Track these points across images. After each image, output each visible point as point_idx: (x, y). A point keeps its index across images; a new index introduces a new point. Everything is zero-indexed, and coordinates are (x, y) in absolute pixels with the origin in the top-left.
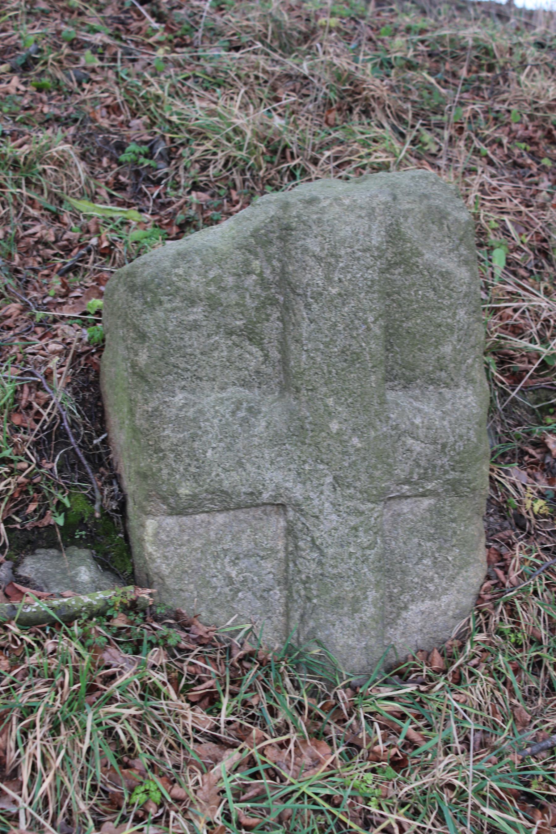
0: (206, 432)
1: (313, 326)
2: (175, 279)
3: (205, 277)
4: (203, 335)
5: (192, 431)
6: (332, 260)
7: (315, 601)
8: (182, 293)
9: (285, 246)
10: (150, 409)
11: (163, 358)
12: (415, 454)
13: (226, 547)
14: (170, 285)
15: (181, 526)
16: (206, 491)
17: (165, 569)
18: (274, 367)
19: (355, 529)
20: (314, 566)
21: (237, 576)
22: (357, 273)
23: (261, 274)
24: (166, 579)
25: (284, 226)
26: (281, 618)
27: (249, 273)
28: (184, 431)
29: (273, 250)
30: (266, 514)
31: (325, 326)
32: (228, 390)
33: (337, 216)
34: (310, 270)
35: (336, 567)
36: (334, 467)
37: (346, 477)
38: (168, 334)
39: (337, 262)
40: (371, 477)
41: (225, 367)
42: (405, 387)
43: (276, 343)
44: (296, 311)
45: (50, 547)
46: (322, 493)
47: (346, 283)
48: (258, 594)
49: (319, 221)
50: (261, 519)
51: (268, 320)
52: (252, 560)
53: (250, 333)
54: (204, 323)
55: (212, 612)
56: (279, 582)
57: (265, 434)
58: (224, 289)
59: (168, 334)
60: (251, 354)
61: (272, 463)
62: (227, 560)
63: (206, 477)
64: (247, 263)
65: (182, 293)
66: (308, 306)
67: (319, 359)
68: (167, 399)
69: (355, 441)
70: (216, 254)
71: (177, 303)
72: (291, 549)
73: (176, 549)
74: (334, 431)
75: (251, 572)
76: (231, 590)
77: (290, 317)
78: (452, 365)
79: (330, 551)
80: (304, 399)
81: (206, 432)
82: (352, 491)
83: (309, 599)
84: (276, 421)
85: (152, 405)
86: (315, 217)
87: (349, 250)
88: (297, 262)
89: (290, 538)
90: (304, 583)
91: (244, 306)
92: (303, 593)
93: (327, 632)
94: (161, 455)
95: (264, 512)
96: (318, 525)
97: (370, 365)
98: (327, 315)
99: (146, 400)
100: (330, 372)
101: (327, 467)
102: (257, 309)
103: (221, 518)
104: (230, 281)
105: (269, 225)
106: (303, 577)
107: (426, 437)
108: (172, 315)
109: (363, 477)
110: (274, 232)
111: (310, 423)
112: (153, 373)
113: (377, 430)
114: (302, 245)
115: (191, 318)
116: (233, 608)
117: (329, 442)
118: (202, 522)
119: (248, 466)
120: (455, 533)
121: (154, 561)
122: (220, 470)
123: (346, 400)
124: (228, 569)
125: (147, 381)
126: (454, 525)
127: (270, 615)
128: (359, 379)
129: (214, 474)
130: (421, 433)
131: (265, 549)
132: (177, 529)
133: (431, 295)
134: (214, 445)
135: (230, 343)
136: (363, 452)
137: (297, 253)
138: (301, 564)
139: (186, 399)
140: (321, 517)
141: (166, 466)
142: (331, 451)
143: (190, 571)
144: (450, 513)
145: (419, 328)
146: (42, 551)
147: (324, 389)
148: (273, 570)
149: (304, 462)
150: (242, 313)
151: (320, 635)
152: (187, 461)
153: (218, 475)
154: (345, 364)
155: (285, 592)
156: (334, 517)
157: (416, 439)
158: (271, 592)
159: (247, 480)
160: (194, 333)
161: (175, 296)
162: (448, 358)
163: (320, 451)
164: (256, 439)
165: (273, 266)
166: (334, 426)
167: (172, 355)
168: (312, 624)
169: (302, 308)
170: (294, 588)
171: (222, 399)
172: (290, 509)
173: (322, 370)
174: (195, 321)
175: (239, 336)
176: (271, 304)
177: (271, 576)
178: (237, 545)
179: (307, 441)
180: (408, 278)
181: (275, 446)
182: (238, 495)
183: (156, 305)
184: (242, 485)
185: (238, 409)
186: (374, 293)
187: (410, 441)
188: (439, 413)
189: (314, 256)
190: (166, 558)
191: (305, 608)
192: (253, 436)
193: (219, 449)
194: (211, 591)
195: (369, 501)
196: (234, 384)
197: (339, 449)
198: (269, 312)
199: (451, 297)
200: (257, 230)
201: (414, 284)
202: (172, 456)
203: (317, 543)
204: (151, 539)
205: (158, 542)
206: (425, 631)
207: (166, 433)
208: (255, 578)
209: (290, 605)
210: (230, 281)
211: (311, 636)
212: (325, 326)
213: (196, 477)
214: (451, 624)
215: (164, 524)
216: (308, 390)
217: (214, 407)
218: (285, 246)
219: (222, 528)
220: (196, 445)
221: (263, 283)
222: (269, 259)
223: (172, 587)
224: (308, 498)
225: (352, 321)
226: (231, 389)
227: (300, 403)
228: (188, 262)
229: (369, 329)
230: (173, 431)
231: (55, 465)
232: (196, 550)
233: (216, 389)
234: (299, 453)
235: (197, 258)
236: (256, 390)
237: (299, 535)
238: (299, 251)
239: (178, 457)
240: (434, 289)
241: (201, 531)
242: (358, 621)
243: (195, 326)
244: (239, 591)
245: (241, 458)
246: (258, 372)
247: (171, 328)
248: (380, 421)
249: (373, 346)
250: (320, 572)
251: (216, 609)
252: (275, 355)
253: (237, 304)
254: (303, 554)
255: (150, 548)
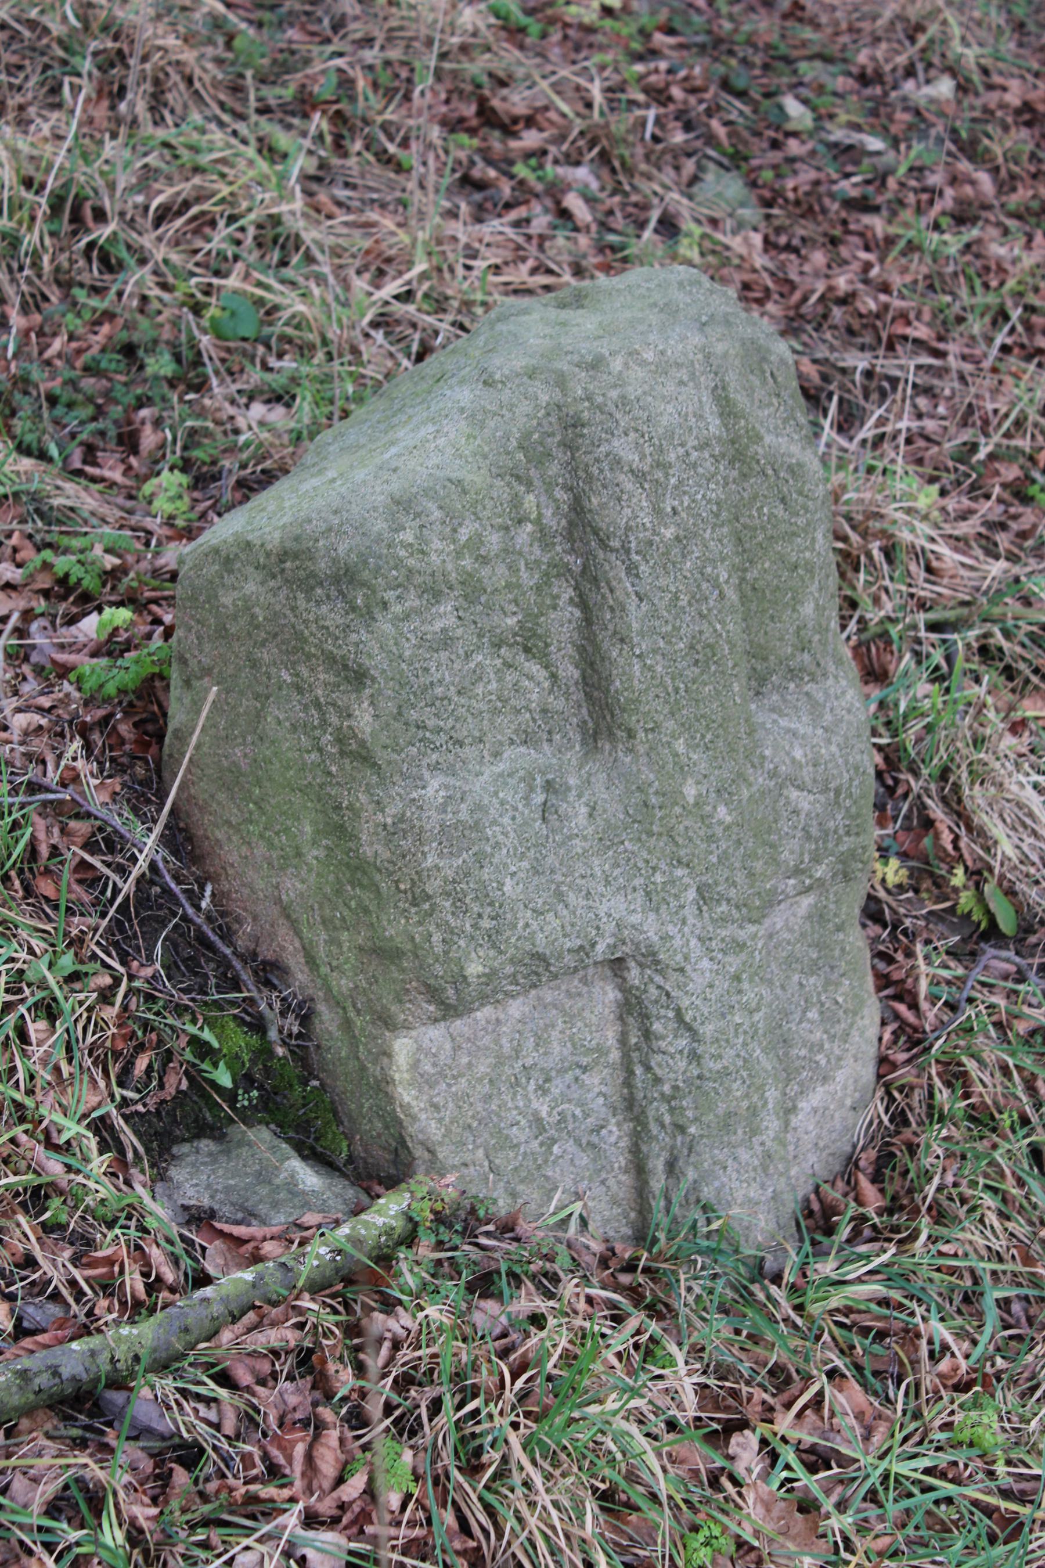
0: (497, 845)
1: (645, 607)
2: (403, 553)
3: (454, 542)
4: (458, 656)
5: (475, 849)
6: (659, 475)
7: (692, 1130)
8: (418, 580)
9: (573, 458)
10: (389, 821)
11: (400, 714)
12: (803, 816)
13: (529, 1062)
14: (396, 568)
15: (453, 1040)
16: (512, 961)
17: (434, 1131)
18: (567, 695)
19: (737, 978)
20: (682, 1064)
21: (550, 1114)
22: (697, 493)
23: (538, 521)
24: (438, 1149)
25: (570, 421)
26: (623, 1178)
27: (520, 522)
28: (460, 851)
29: (554, 469)
30: (586, 984)
31: (662, 602)
32: (505, 755)
33: (646, 387)
34: (629, 500)
35: (720, 1057)
36: (698, 869)
37: (716, 884)
38: (404, 666)
39: (667, 475)
40: (751, 875)
41: (495, 712)
42: (758, 693)
43: (570, 650)
44: (614, 583)
45: (198, 1136)
46: (684, 922)
47: (684, 515)
48: (584, 1141)
49: (623, 402)
50: (579, 995)
51: (555, 608)
52: (569, 1076)
53: (526, 639)
54: (459, 632)
55: (514, 1195)
56: (615, 1109)
57: (590, 830)
58: (484, 560)
59: (404, 666)
60: (530, 678)
61: (608, 883)
62: (532, 1086)
63: (509, 933)
64: (516, 502)
65: (418, 580)
66: (632, 570)
67: (659, 668)
68: (414, 795)
69: (722, 811)
70: (465, 492)
71: (413, 601)
72: (634, 1040)
73: (449, 1085)
74: (691, 800)
75: (570, 1101)
76: (541, 1145)
77: (603, 596)
78: (817, 637)
79: (707, 1030)
80: (642, 749)
81: (497, 845)
82: (724, 907)
83: (682, 1129)
84: (605, 801)
85: (391, 810)
86: (614, 394)
87: (681, 451)
88: (605, 487)
89: (630, 1020)
90: (666, 1099)
91: (519, 586)
92: (667, 1119)
93: (717, 1184)
94: (426, 906)
95: (584, 981)
96: (686, 985)
97: (730, 664)
98: (662, 582)
99: (378, 803)
100: (677, 690)
101: (687, 871)
102: (538, 589)
103: (516, 1008)
104: (494, 540)
105: (545, 422)
106: (667, 1088)
107: (815, 781)
108: (405, 627)
109: (740, 877)
110: (552, 435)
111: (657, 793)
112: (385, 747)
113: (750, 785)
114: (607, 455)
115: (438, 625)
116: (547, 1178)
117: (686, 823)
118: (488, 1022)
119: (572, 898)
120: (843, 950)
121: (414, 1118)
122: (529, 913)
123: (703, 736)
124: (535, 1105)
125: (375, 764)
126: (841, 936)
127: (604, 1175)
128: (718, 693)
129: (520, 925)
130: (807, 774)
131: (591, 1050)
132: (448, 1046)
133: (780, 511)
134: (513, 869)
135: (498, 662)
136: (735, 829)
137: (601, 471)
138: (660, 1065)
139: (447, 787)
140: (688, 968)
141: (438, 926)
142: (690, 840)
143: (475, 1124)
144: (836, 915)
145: (769, 578)
146: (185, 1148)
147: (670, 725)
148: (604, 1089)
149: (654, 869)
150: (516, 602)
151: (707, 1193)
152: (476, 908)
153: (527, 925)
154: (697, 670)
155: (628, 1126)
156: (705, 964)
157: (800, 788)
158: (604, 1132)
159: (573, 925)
160: (444, 655)
161: (406, 588)
162: (810, 625)
163: (676, 844)
164: (576, 841)
165: (556, 500)
166: (690, 791)
167: (413, 706)
168: (691, 1174)
169: (623, 575)
170: (651, 1114)
171: (501, 775)
172: (633, 964)
173: (666, 688)
174: (444, 630)
175: (511, 646)
176: (558, 576)
177: (601, 1100)
178: (545, 1054)
179: (655, 829)
180: (746, 485)
181: (609, 848)
182: (560, 957)
183: (376, 610)
184: (565, 936)
185: (532, 789)
186: (722, 525)
187: (794, 794)
188: (820, 732)
189: (632, 471)
190: (436, 1107)
191: (673, 1147)
192: (570, 838)
193: (522, 875)
194: (512, 1155)
195: (750, 921)
196: (512, 742)
197: (702, 833)
198: (555, 591)
199: (807, 511)
200: (527, 435)
201: (755, 497)
202: (448, 904)
203: (688, 1019)
204: (406, 1076)
205: (424, 1082)
206: (821, 1144)
207: (430, 861)
208: (578, 1112)
209: (644, 1148)
210: (494, 540)
211: (692, 1199)
212: (662, 602)
213: (493, 938)
214: (850, 1122)
215: (426, 1043)
216: (646, 731)
217: (496, 793)
218: (573, 458)
219: (519, 1026)
220: (486, 874)
221: (543, 537)
222: (549, 487)
223: (450, 1162)
224: (666, 938)
225: (699, 586)
226: (508, 753)
227: (636, 760)
228: (418, 515)
229: (722, 596)
230: (441, 855)
231: (158, 966)
232: (480, 1080)
233: (487, 758)
234: (645, 854)
235: (432, 506)
236: (546, 746)
237: (653, 1010)
238: (605, 465)
239: (460, 906)
240: (783, 500)
241: (487, 1040)
242: (759, 1149)
243: (446, 641)
244: (554, 1141)
245: (559, 885)
246: (544, 711)
247: (407, 653)
248: (753, 766)
249: (731, 627)
250: (696, 1073)
251: (521, 1188)
252: (569, 672)
253: (509, 586)
254: (662, 1044)
255: (405, 1095)
